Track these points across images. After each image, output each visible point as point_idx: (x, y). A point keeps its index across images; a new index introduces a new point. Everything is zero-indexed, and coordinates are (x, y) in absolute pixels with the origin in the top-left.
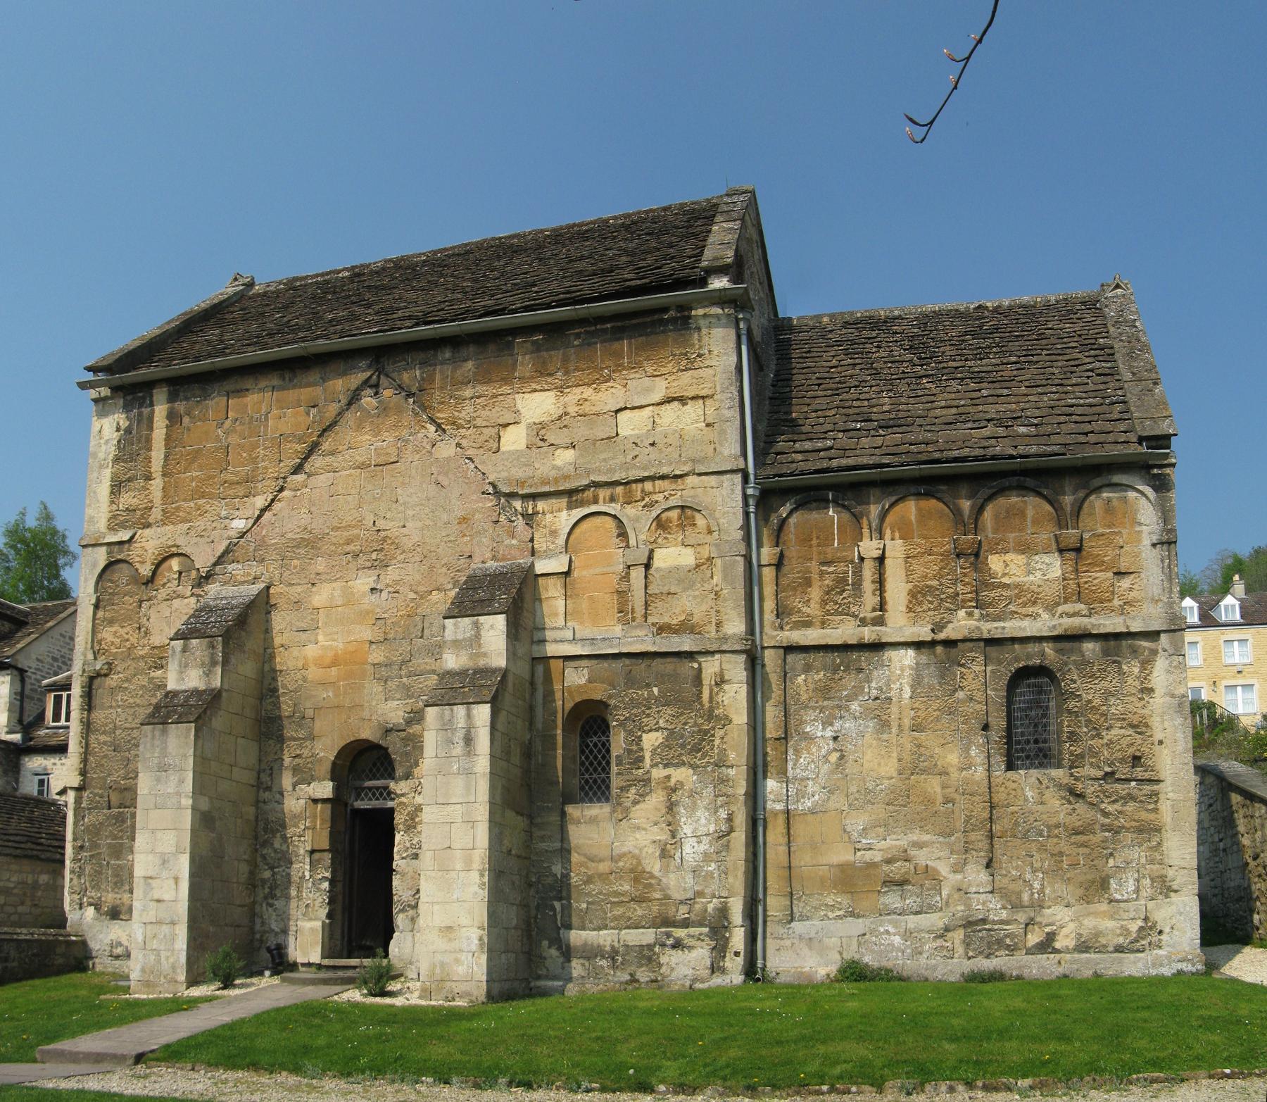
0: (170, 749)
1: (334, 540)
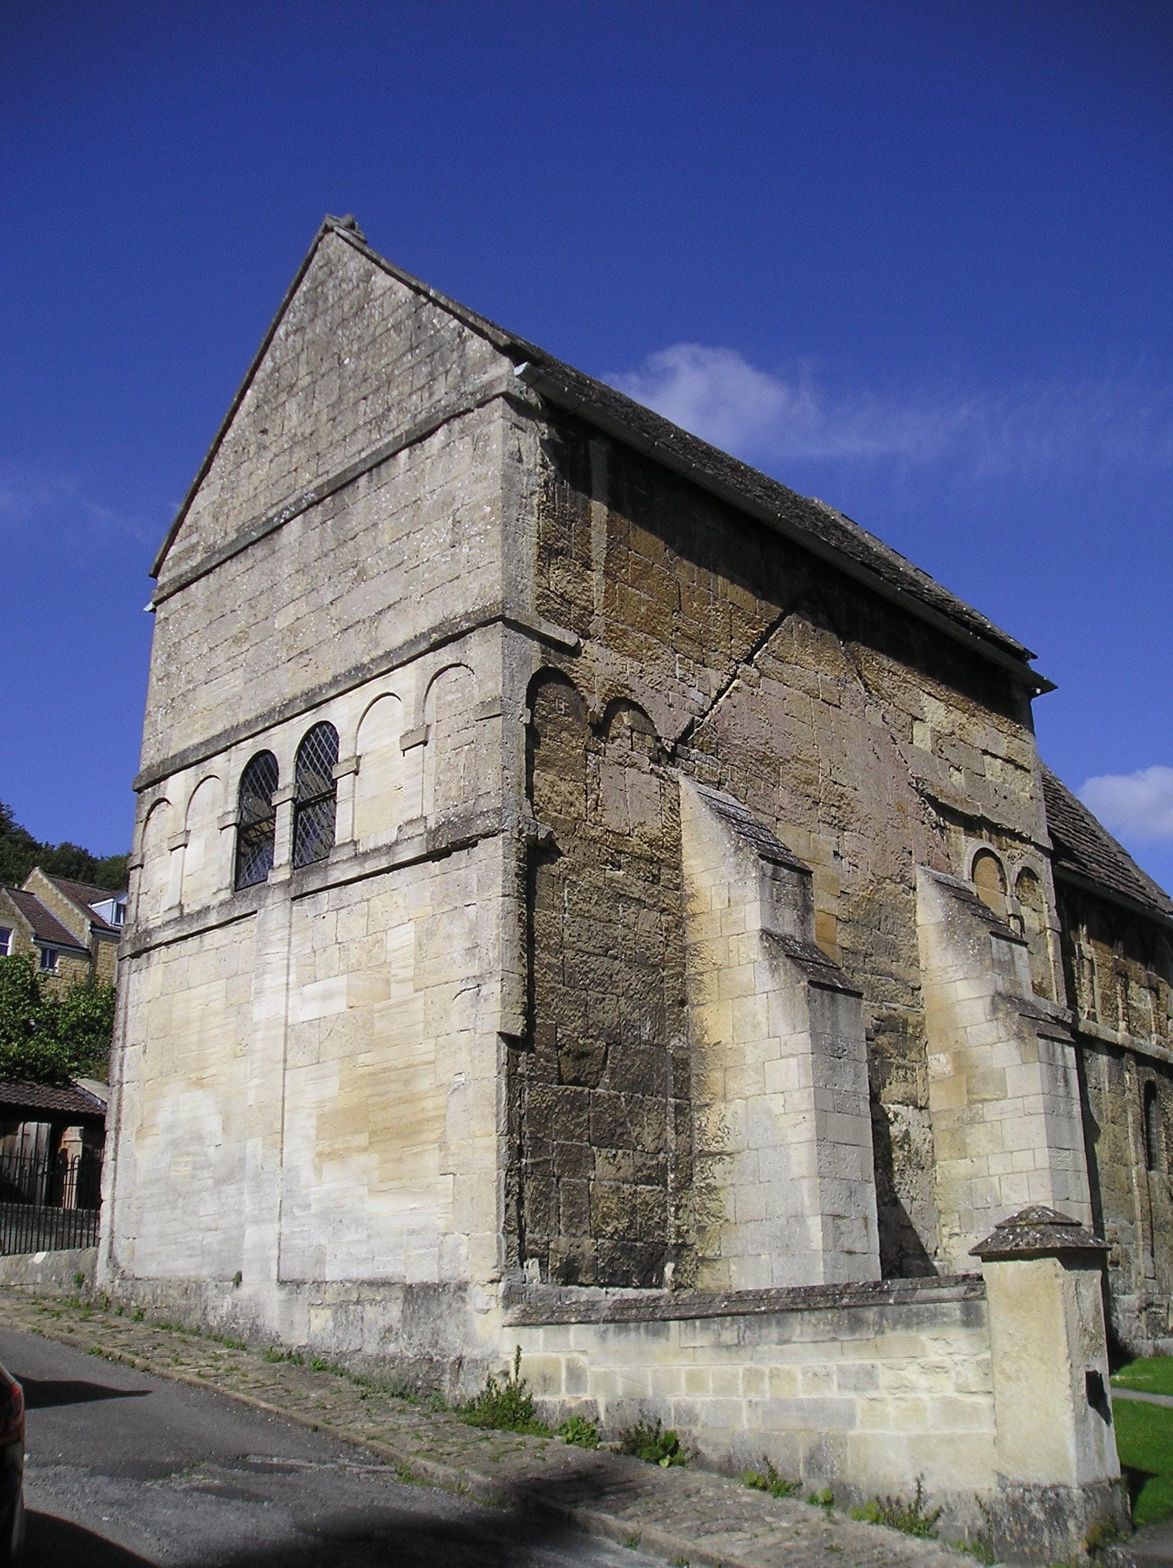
0: (841, 1027)
1: (796, 773)
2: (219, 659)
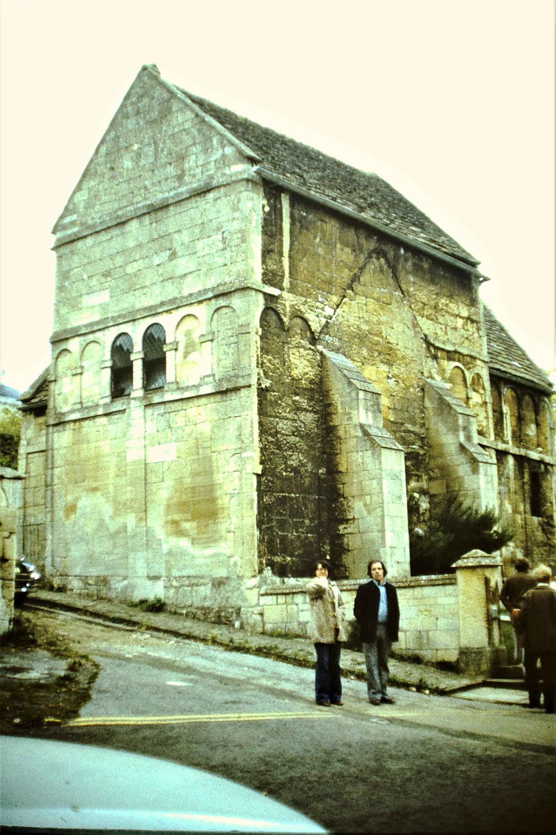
2: (94, 282)
